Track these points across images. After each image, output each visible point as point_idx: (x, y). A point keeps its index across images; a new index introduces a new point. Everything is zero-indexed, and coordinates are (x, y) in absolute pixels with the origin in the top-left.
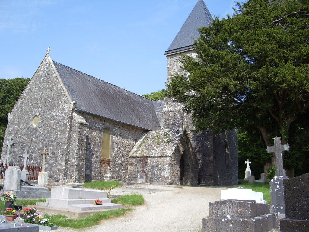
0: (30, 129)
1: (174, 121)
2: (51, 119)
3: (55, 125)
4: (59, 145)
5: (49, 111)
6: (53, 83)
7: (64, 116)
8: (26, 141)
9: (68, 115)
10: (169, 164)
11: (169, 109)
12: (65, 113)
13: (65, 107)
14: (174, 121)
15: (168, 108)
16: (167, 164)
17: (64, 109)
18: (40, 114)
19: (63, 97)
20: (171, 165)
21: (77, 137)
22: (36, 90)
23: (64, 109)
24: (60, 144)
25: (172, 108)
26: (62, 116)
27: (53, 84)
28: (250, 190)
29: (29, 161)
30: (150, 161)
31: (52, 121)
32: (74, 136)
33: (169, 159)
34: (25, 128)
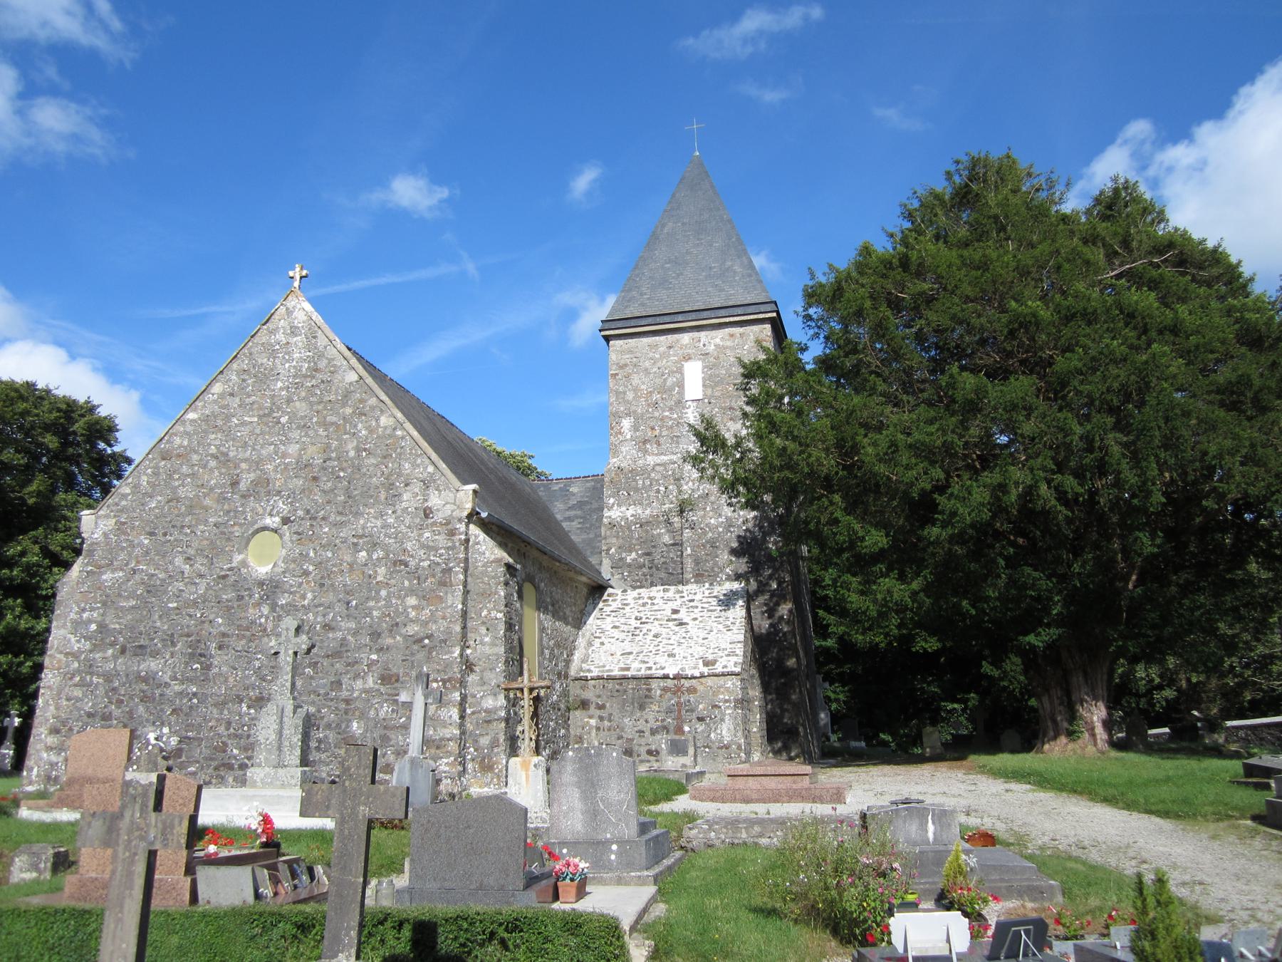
0: (237, 582)
1: (648, 554)
2: (355, 544)
3: (382, 571)
4: (415, 647)
5: (340, 513)
6: (344, 405)
7: (427, 535)
8: (214, 631)
9: (452, 533)
10: (736, 701)
11: (629, 513)
12: (434, 524)
13: (429, 504)
14: (648, 554)
15: (624, 509)
16: (726, 701)
17: (427, 513)
18: (286, 521)
19: (415, 465)
20: (743, 703)
21: (500, 615)
22: (248, 428)
23: (425, 510)
24: (421, 640)
25: (640, 511)
26: (420, 535)
27: (349, 411)
28: (1001, 755)
29: (245, 709)
30: (659, 692)
31: (364, 554)
32: (485, 613)
33: (730, 683)
34: (201, 576)
